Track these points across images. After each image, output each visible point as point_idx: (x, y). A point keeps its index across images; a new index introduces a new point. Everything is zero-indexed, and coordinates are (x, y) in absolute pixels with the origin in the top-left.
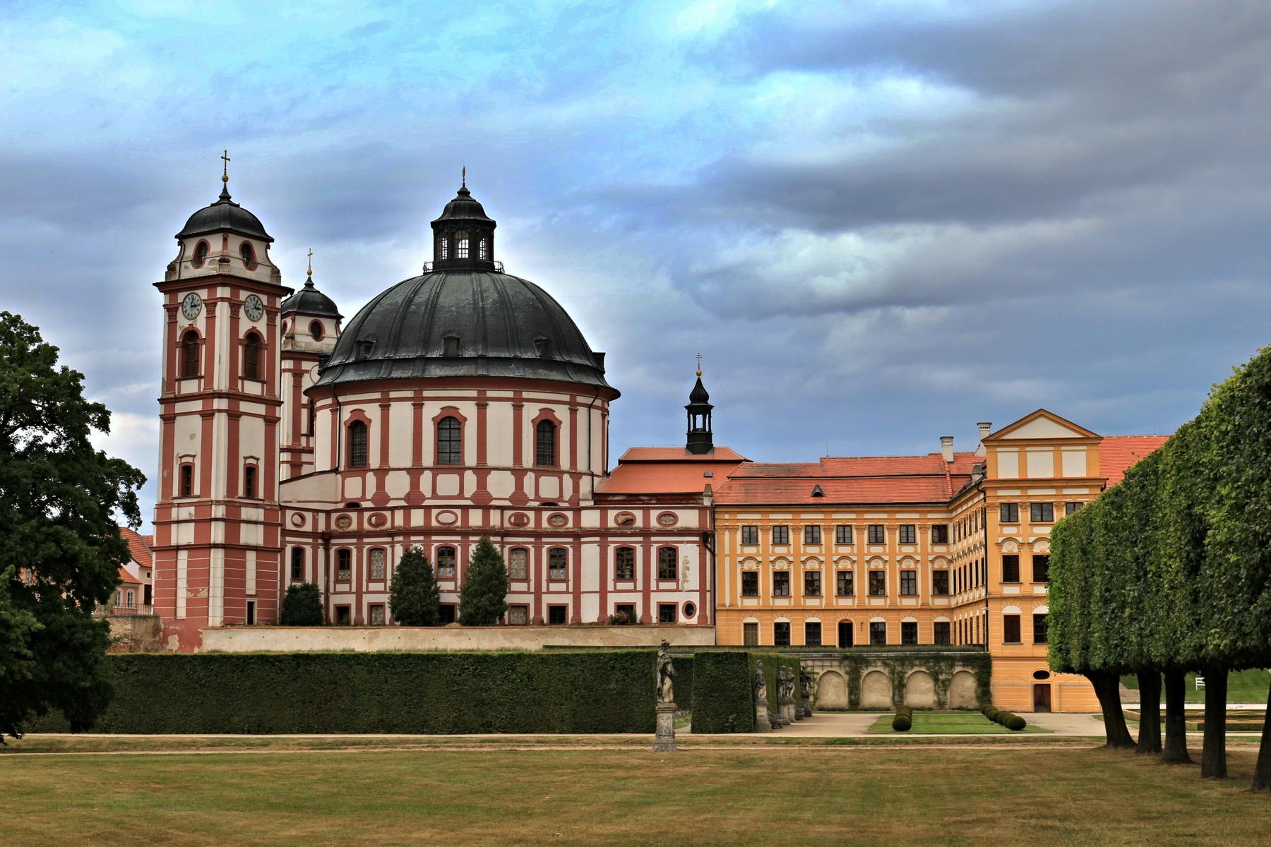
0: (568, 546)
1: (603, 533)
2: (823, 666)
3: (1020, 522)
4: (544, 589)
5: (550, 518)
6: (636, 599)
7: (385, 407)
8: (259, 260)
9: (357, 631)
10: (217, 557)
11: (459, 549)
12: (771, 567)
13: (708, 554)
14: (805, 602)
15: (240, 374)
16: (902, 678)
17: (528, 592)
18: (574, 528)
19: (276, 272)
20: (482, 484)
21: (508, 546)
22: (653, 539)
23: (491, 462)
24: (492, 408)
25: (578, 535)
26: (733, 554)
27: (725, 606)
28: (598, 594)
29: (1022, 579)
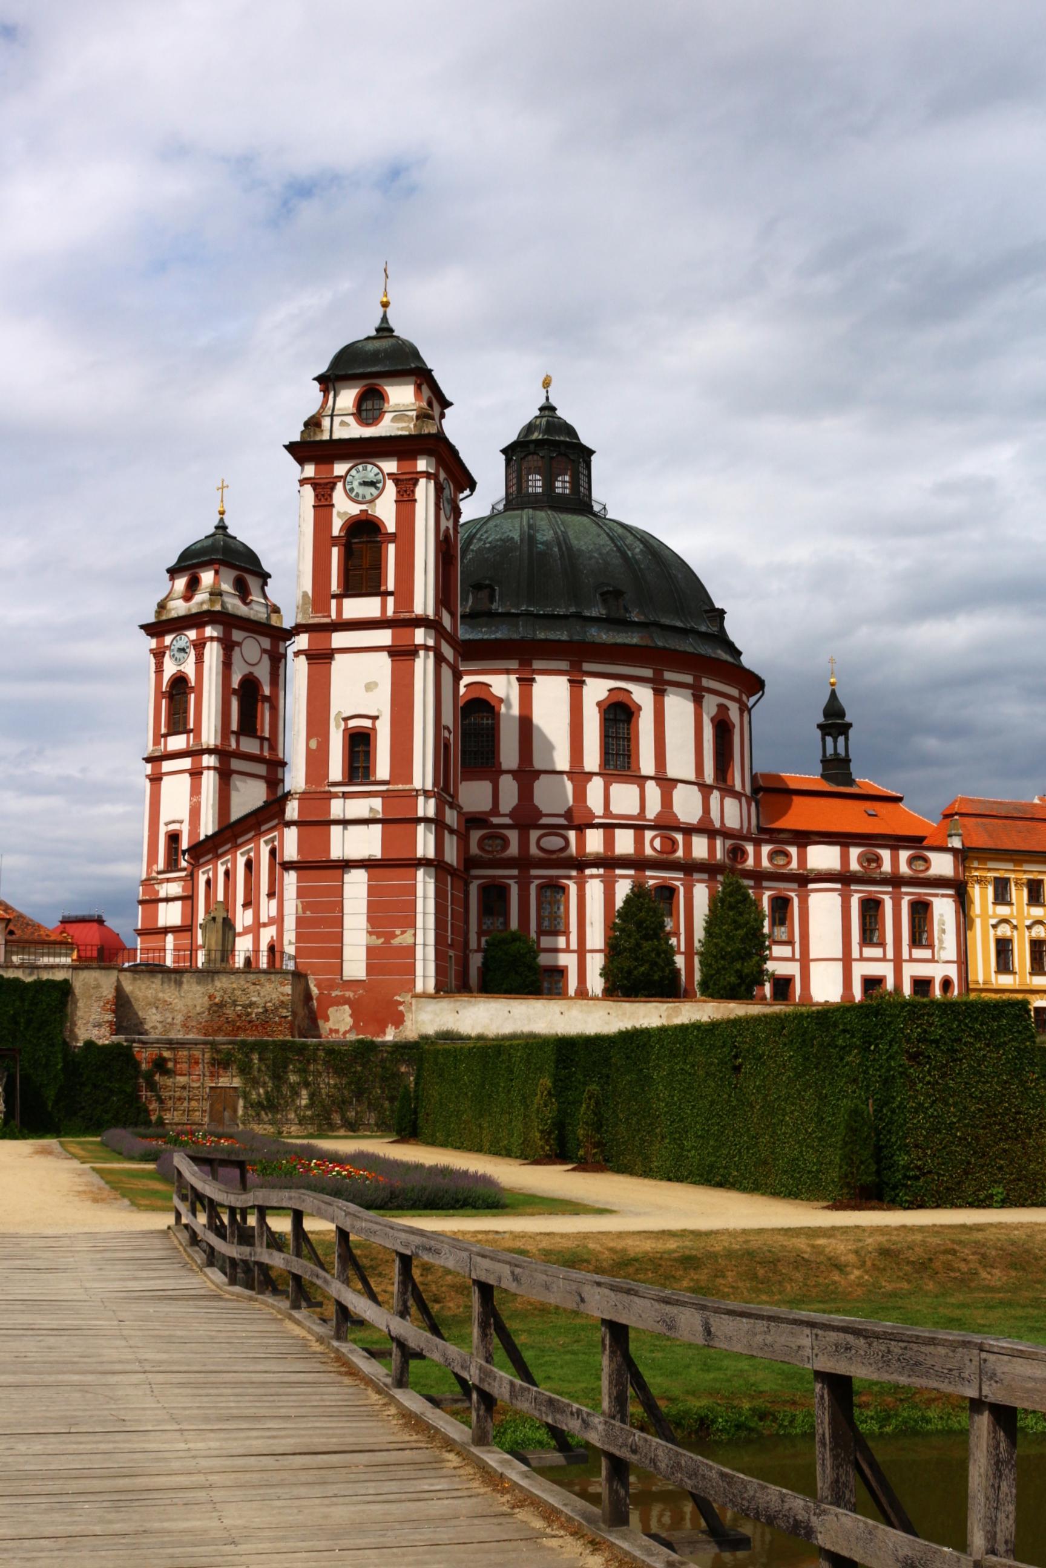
0: (793, 894)
1: (844, 879)
6: (885, 970)
7: (526, 683)
9: (650, 1005)
10: (425, 885)
11: (682, 889)
18: (799, 867)
20: (667, 801)
22: (904, 889)
25: (804, 879)
26: (984, 915)
27: (977, 983)
28: (840, 964)
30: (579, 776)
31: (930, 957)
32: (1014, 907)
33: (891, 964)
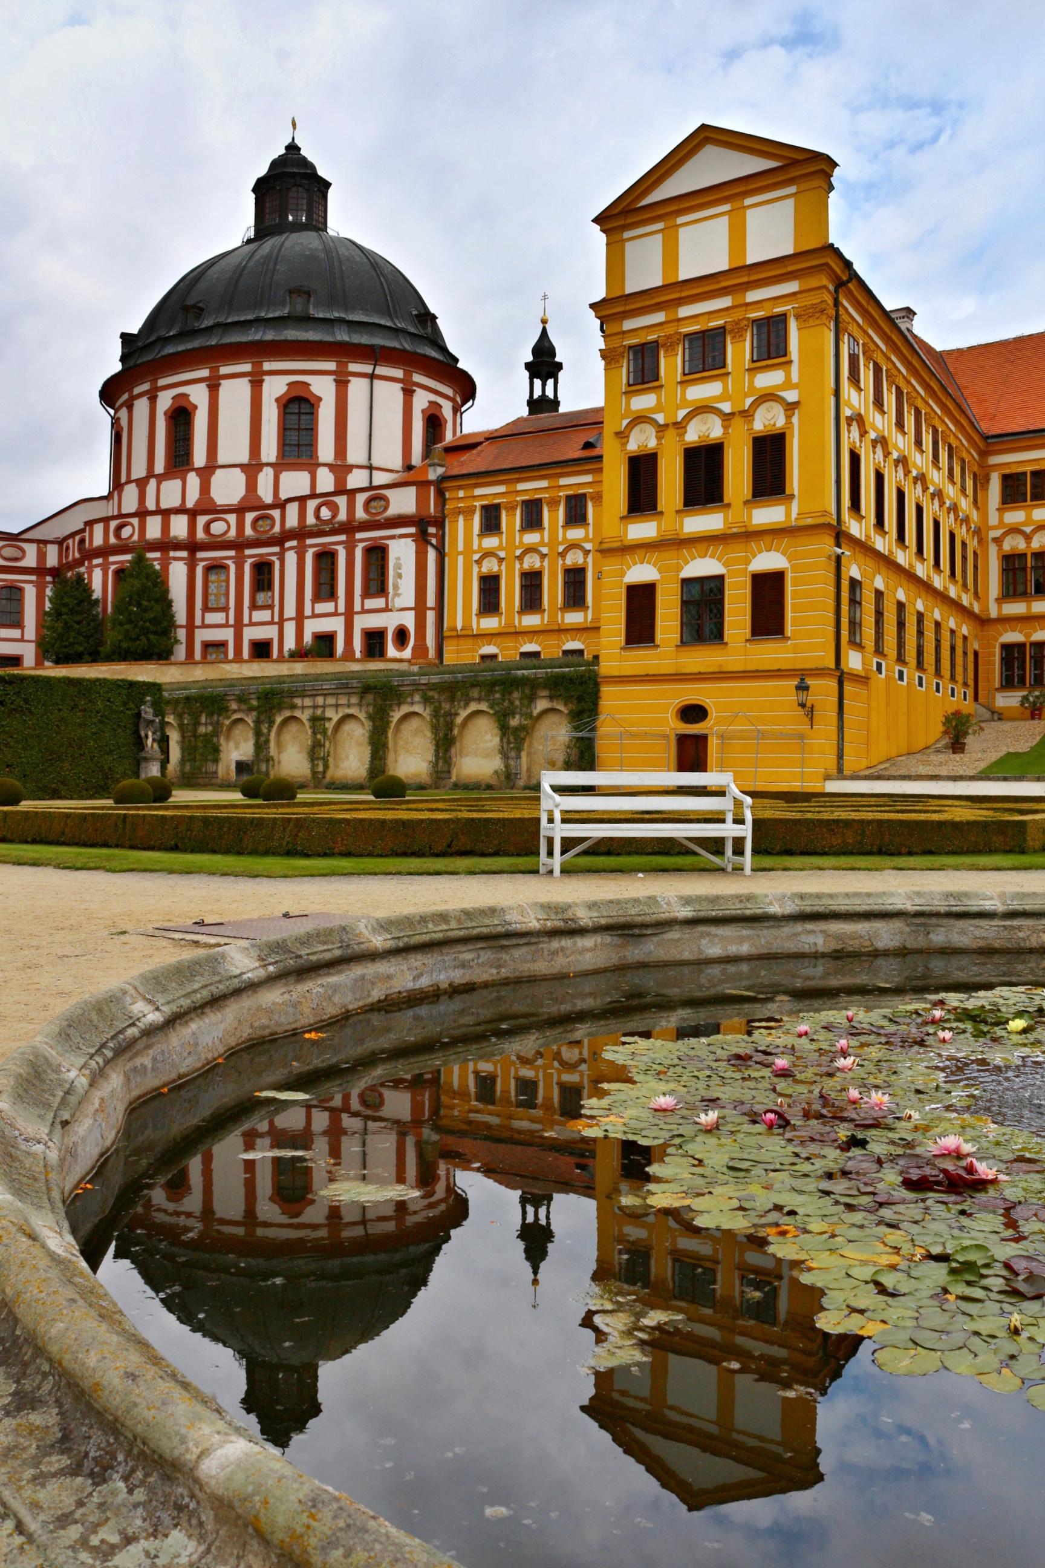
0: (274, 558)
1: (301, 534)
2: (337, 706)
3: (663, 379)
4: (246, 621)
5: (255, 521)
6: (336, 625)
12: (517, 566)
13: (432, 554)
14: (563, 618)
16: (450, 726)
20: (205, 488)
21: (202, 564)
23: (222, 459)
26: (468, 549)
27: (455, 629)
29: (663, 503)
30: (142, 483)
32: (504, 536)
33: (342, 619)
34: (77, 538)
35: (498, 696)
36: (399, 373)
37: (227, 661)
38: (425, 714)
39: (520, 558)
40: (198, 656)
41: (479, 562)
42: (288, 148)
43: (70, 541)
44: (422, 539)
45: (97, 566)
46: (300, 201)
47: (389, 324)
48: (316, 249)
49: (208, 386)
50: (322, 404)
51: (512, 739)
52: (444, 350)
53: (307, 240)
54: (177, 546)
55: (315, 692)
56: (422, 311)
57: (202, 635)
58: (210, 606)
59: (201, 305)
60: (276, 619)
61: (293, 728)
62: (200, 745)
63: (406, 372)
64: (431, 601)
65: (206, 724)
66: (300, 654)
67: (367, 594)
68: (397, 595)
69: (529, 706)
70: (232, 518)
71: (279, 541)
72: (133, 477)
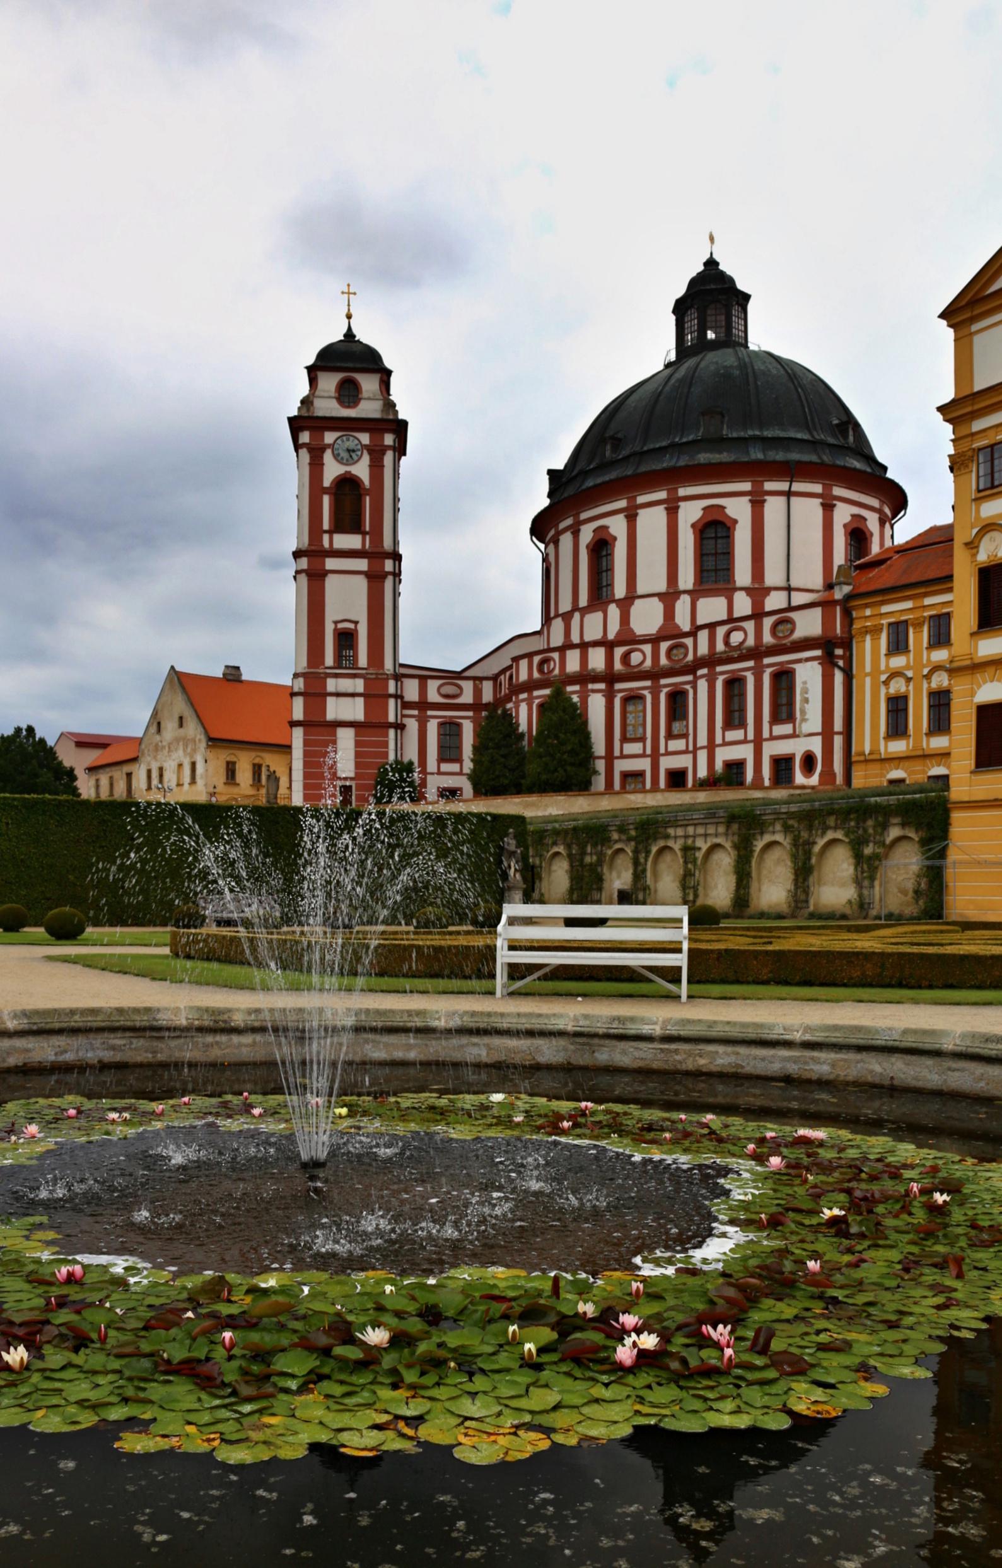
0: (688, 687)
1: (712, 661)
2: (706, 835)
5: (670, 650)
6: (745, 752)
8: (365, 394)
13: (839, 677)
15: (326, 526)
16: (808, 854)
17: (643, 755)
19: (390, 406)
20: (625, 619)
21: (620, 695)
23: (641, 589)
24: (644, 516)
27: (863, 754)
30: (567, 617)
31: (791, 731)
32: (911, 655)
34: (508, 674)
35: (852, 824)
36: (817, 488)
37: (643, 791)
38: (785, 843)
39: (928, 677)
40: (617, 786)
41: (886, 683)
42: (706, 264)
43: (502, 677)
44: (828, 662)
45: (523, 700)
46: (718, 318)
47: (806, 437)
48: (731, 367)
49: (626, 517)
50: (738, 526)
51: (865, 867)
52: (870, 459)
53: (725, 358)
54: (596, 678)
55: (685, 822)
56: (845, 419)
57: (621, 766)
58: (628, 736)
59: (619, 435)
60: (691, 748)
61: (668, 857)
62: (586, 874)
63: (827, 488)
64: (838, 725)
65: (591, 854)
66: (711, 783)
67: (776, 719)
68: (804, 720)
69: (882, 834)
70: (647, 648)
71: (691, 669)
72: (561, 611)
